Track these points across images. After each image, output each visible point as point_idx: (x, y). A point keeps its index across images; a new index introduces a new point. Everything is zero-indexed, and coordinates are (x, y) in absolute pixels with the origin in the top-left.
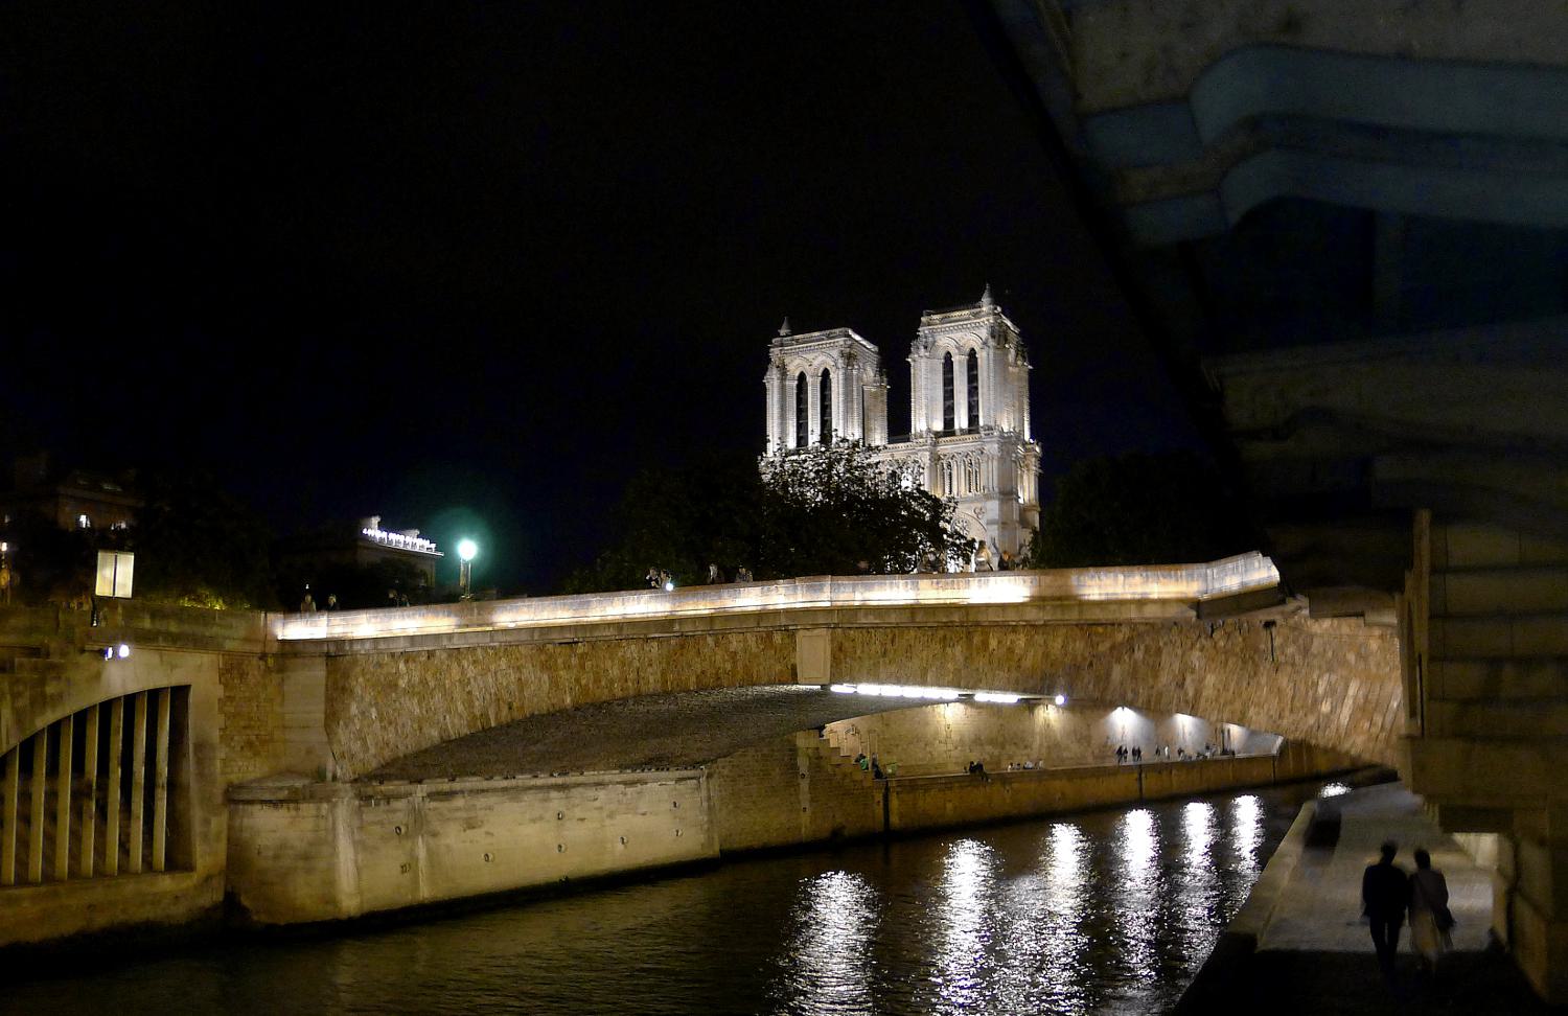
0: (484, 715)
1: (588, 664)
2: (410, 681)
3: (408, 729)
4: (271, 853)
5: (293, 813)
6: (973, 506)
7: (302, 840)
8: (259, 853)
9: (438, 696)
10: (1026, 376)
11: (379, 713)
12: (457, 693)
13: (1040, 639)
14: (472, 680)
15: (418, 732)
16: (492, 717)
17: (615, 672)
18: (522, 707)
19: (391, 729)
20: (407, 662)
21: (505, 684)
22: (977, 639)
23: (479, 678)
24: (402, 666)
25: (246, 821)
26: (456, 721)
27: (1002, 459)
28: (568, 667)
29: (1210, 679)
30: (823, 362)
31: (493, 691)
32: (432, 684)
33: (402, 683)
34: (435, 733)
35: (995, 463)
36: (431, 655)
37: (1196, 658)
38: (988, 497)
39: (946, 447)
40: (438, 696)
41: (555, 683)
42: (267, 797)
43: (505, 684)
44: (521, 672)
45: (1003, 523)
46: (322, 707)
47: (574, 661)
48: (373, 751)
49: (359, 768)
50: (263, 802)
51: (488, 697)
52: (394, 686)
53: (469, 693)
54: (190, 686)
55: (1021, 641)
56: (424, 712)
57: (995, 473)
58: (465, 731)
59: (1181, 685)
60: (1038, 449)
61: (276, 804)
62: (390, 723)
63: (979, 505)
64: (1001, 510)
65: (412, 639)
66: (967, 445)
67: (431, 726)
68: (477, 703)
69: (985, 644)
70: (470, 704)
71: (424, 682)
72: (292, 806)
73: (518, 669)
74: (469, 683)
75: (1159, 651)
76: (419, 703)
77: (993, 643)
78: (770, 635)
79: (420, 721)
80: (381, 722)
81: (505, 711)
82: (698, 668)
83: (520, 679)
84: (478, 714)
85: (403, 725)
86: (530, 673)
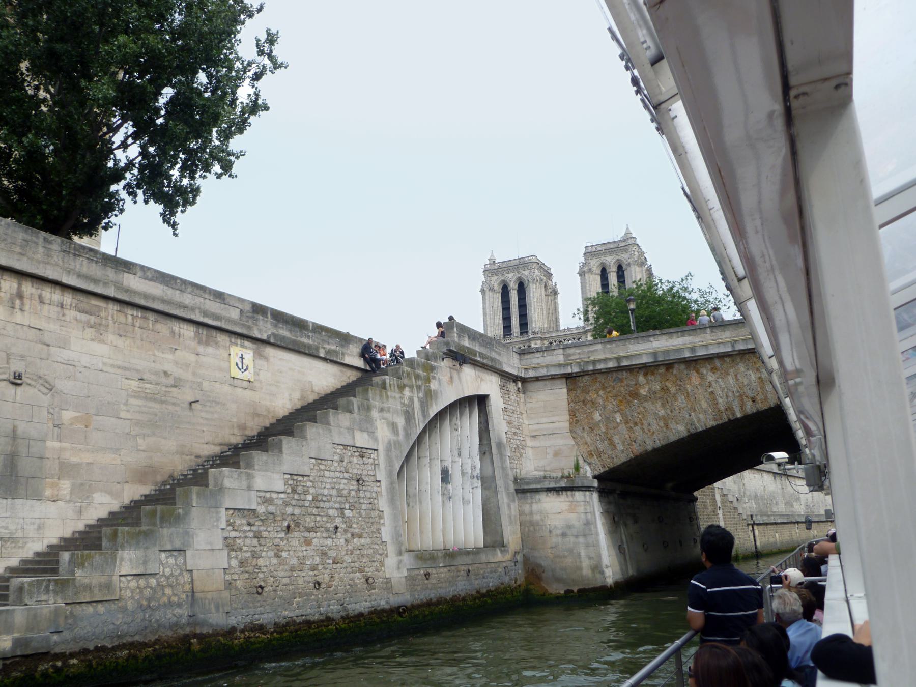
0: (729, 408)
2: (650, 389)
3: (654, 427)
4: (559, 532)
5: (571, 499)
7: (579, 521)
8: (550, 532)
9: (681, 398)
14: (713, 383)
15: (665, 429)
18: (766, 398)
19: (637, 428)
20: (645, 375)
21: (745, 383)
23: (720, 380)
25: (535, 507)
26: (701, 416)
30: (519, 278)
31: (735, 390)
32: (673, 390)
33: (643, 392)
40: (681, 398)
42: (552, 485)
43: (745, 383)
44: (760, 372)
46: (567, 417)
48: (620, 447)
49: (610, 464)
50: (549, 490)
51: (730, 394)
52: (635, 395)
53: (712, 393)
54: (488, 396)
56: (669, 412)
58: (711, 423)
61: (557, 490)
62: (636, 424)
67: (677, 423)
68: (720, 400)
71: (664, 389)
72: (569, 493)
73: (758, 370)
74: (710, 385)
76: (663, 405)
79: (665, 420)
80: (627, 423)
83: (760, 378)
84: (722, 408)
85: (649, 424)
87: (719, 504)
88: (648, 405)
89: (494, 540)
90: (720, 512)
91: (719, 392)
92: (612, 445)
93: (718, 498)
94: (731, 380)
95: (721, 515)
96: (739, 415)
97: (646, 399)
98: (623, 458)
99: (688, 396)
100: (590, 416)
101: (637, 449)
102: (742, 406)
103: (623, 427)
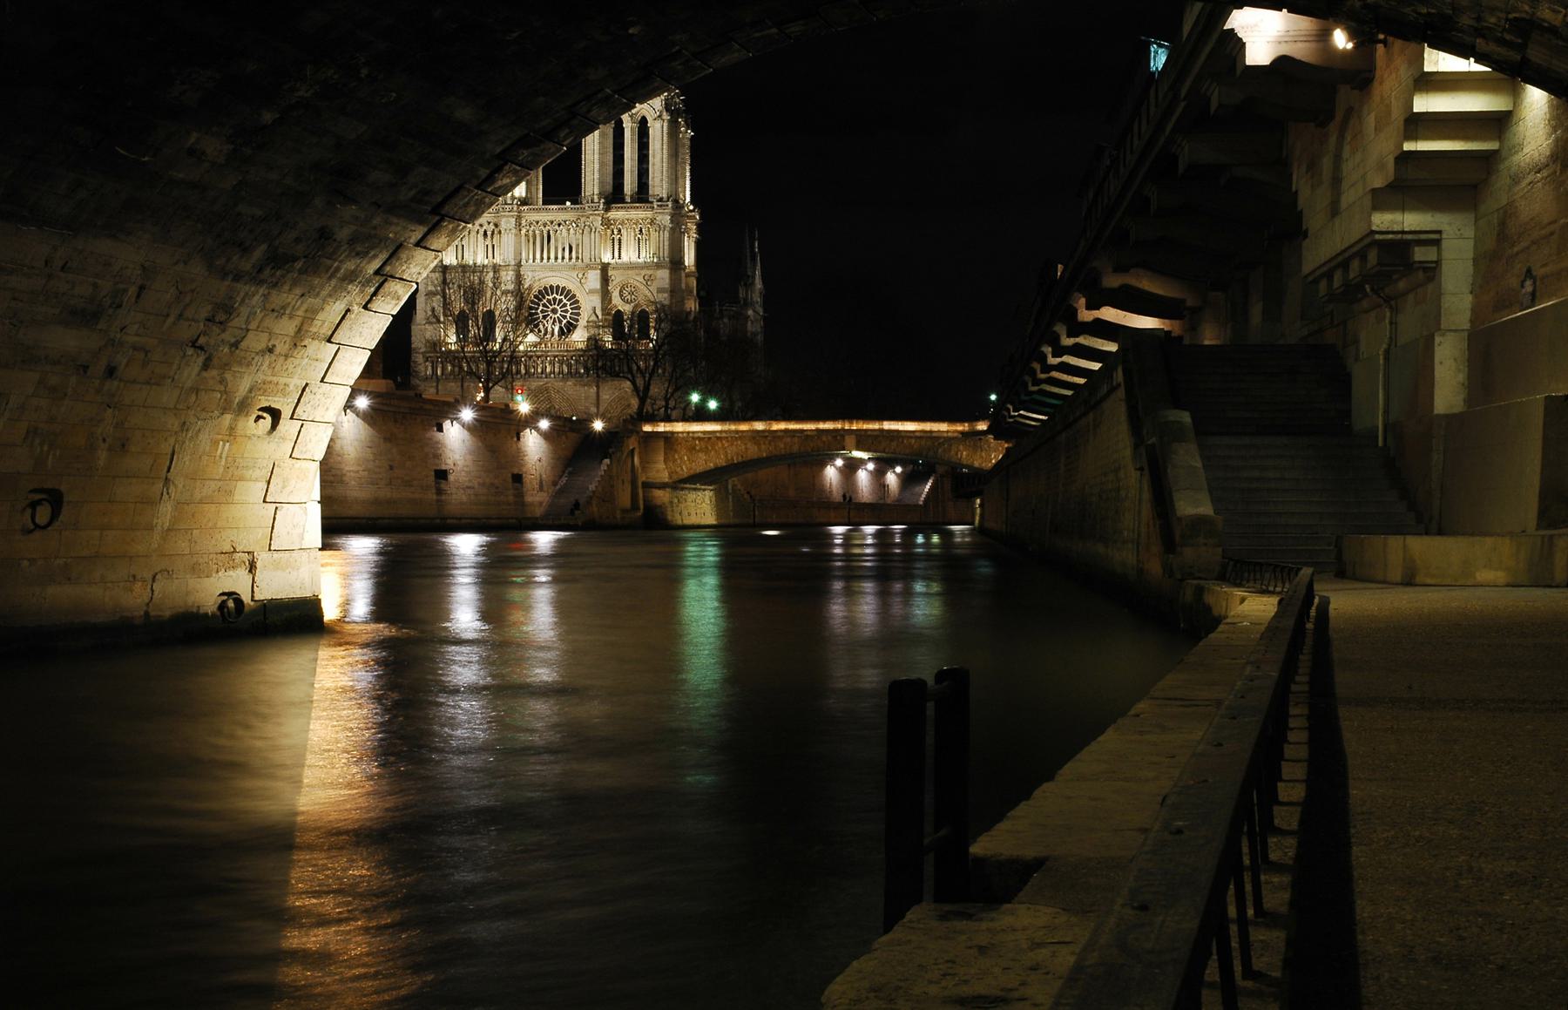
1: (773, 444)
6: (643, 272)
10: (688, 143)
11: (688, 457)
12: (721, 452)
13: (918, 440)
16: (735, 458)
17: (782, 446)
22: (900, 440)
24: (697, 442)
27: (672, 230)
28: (764, 444)
29: (964, 453)
32: (710, 448)
33: (697, 448)
34: (712, 465)
35: (667, 234)
36: (710, 438)
37: (961, 447)
38: (658, 266)
39: (616, 214)
41: (760, 449)
45: (671, 291)
47: (767, 442)
52: (694, 448)
55: (913, 441)
57: (667, 243)
58: (724, 464)
59: (957, 454)
60: (698, 217)
63: (649, 272)
64: (671, 279)
65: (704, 432)
66: (639, 214)
69: (903, 442)
70: (726, 456)
71: (707, 448)
73: (746, 444)
75: (951, 445)
77: (905, 441)
78: (836, 437)
80: (689, 460)
81: (740, 458)
82: (812, 445)
86: (749, 445)
87: (730, 491)
88: (700, 455)
89: (635, 506)
90: (730, 497)
91: (729, 452)
92: (682, 468)
93: (730, 487)
94: (734, 447)
95: (730, 500)
96: (735, 462)
97: (699, 451)
98: (686, 476)
99: (716, 451)
100: (674, 456)
101: (692, 472)
102: (737, 458)
103: (687, 462)
